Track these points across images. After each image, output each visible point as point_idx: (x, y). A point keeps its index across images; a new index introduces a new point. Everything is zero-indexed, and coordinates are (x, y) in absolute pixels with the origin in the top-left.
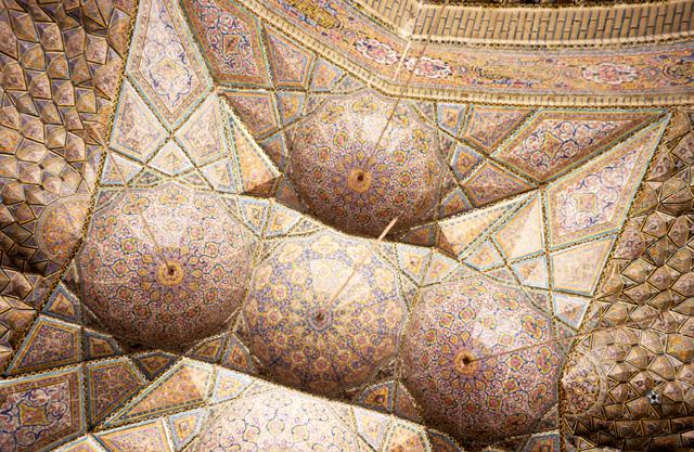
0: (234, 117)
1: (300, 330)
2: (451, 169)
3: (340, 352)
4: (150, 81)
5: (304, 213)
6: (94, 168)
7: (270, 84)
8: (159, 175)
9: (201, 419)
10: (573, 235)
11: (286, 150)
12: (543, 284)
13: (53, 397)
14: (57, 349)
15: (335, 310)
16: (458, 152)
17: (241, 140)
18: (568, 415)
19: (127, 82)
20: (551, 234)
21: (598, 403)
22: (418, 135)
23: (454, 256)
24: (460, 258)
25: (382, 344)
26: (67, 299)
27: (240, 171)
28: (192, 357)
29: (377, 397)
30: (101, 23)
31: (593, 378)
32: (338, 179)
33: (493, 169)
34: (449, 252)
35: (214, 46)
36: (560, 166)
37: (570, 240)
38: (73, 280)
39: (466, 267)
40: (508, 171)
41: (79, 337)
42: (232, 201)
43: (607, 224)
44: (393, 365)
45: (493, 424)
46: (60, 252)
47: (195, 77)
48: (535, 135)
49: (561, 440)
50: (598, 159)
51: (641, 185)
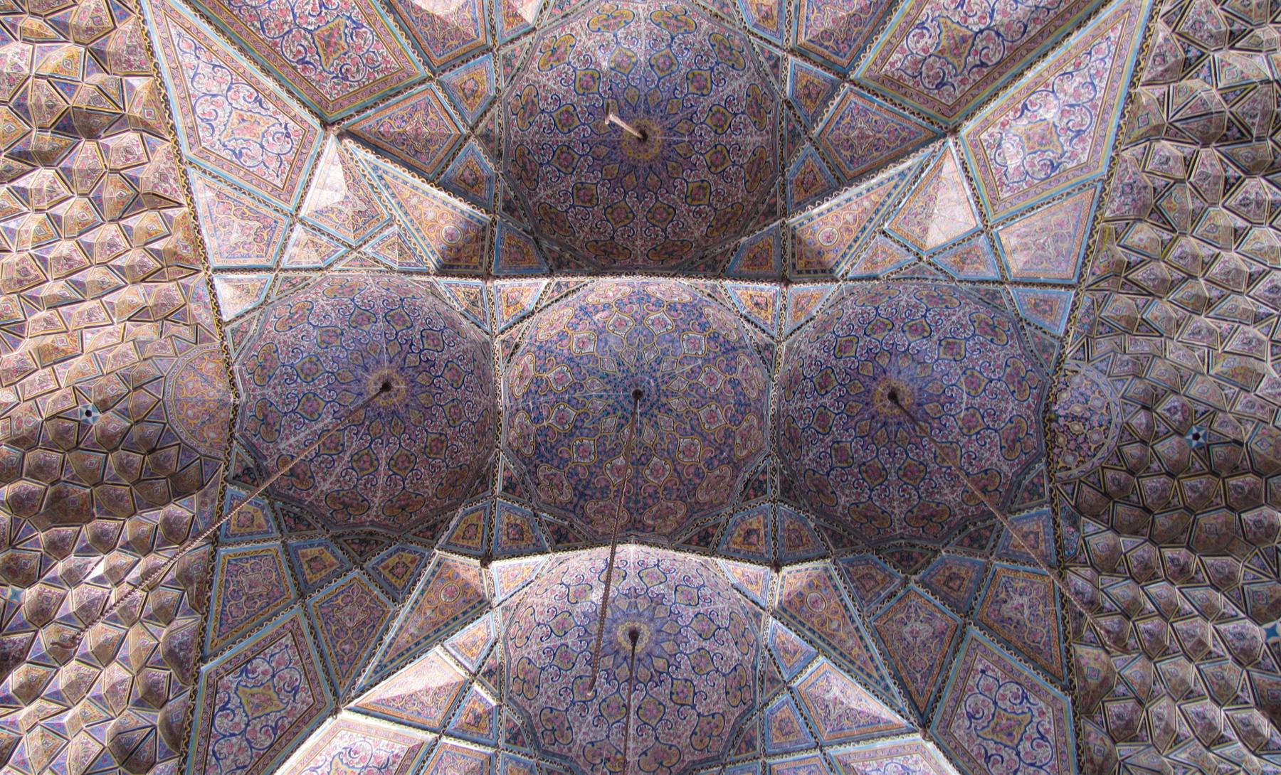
0: (380, 162)
1: (611, 422)
2: (790, 107)
3: (684, 442)
4: (226, 154)
5: (550, 274)
6: (206, 307)
7: (423, 71)
8: (304, 274)
9: (492, 624)
10: (1025, 194)
11: (491, 165)
12: (992, 274)
13: (279, 664)
14: (259, 589)
15: (659, 374)
16: (795, 74)
17: (407, 192)
18: (1062, 474)
19: (191, 171)
20: (986, 199)
21: (1111, 442)
22: (720, 42)
23: (824, 272)
24: (839, 272)
25: (745, 424)
26: (247, 504)
27: (423, 238)
28: (450, 547)
29: (749, 533)
30: (113, 109)
31: (1098, 403)
32: (603, 150)
33: (860, 102)
34: (821, 271)
35: (303, 61)
36: (976, 85)
37: (1022, 204)
38: (247, 470)
39: (851, 283)
40: (888, 104)
41: (282, 558)
42: (431, 283)
43: (1082, 167)
44: (764, 472)
45: (951, 497)
46: (212, 435)
47: (291, 124)
48: (922, 26)
49: (1055, 522)
50: (1041, 66)
51: (1130, 95)
